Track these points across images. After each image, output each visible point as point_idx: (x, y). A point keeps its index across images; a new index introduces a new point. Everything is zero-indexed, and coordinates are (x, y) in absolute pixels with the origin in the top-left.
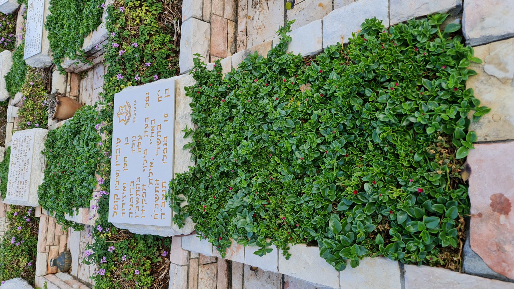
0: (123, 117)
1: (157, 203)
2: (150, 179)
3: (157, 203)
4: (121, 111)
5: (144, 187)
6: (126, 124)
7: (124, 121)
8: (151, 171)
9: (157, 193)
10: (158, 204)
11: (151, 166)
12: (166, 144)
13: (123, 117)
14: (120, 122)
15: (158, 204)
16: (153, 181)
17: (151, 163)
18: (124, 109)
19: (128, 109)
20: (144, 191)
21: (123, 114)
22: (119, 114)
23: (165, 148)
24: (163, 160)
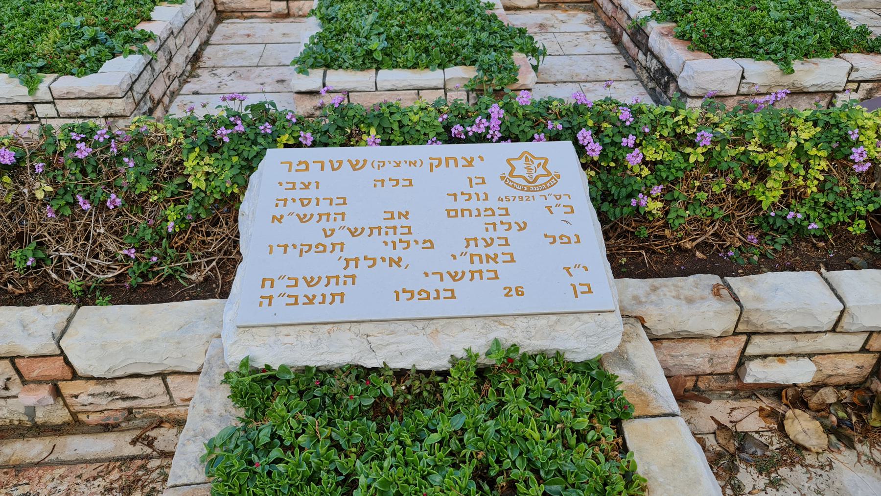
0: (520, 168)
1: (302, 282)
2: (357, 260)
3: (302, 282)
4: (536, 162)
5: (338, 248)
6: (502, 178)
7: (511, 174)
8: (379, 261)
9: (324, 281)
10: (296, 285)
11: (391, 260)
12: (438, 297)
13: (520, 168)
14: (508, 161)
15: (296, 285)
16: (351, 270)
17: (400, 259)
18: (541, 171)
19: (541, 181)
20: (329, 248)
21: (529, 169)
22: (528, 157)
23: (428, 294)
24: (404, 291)
